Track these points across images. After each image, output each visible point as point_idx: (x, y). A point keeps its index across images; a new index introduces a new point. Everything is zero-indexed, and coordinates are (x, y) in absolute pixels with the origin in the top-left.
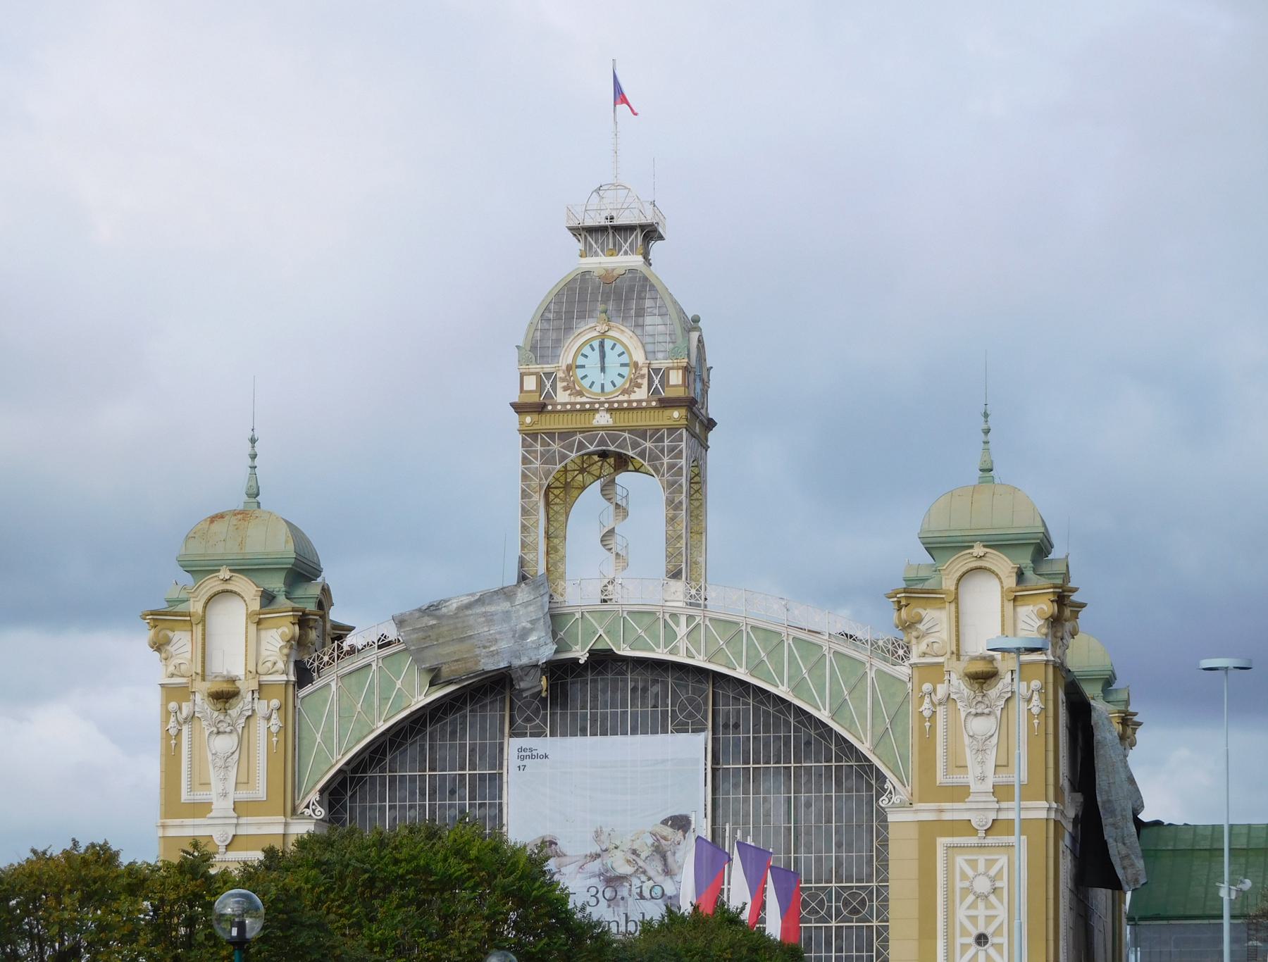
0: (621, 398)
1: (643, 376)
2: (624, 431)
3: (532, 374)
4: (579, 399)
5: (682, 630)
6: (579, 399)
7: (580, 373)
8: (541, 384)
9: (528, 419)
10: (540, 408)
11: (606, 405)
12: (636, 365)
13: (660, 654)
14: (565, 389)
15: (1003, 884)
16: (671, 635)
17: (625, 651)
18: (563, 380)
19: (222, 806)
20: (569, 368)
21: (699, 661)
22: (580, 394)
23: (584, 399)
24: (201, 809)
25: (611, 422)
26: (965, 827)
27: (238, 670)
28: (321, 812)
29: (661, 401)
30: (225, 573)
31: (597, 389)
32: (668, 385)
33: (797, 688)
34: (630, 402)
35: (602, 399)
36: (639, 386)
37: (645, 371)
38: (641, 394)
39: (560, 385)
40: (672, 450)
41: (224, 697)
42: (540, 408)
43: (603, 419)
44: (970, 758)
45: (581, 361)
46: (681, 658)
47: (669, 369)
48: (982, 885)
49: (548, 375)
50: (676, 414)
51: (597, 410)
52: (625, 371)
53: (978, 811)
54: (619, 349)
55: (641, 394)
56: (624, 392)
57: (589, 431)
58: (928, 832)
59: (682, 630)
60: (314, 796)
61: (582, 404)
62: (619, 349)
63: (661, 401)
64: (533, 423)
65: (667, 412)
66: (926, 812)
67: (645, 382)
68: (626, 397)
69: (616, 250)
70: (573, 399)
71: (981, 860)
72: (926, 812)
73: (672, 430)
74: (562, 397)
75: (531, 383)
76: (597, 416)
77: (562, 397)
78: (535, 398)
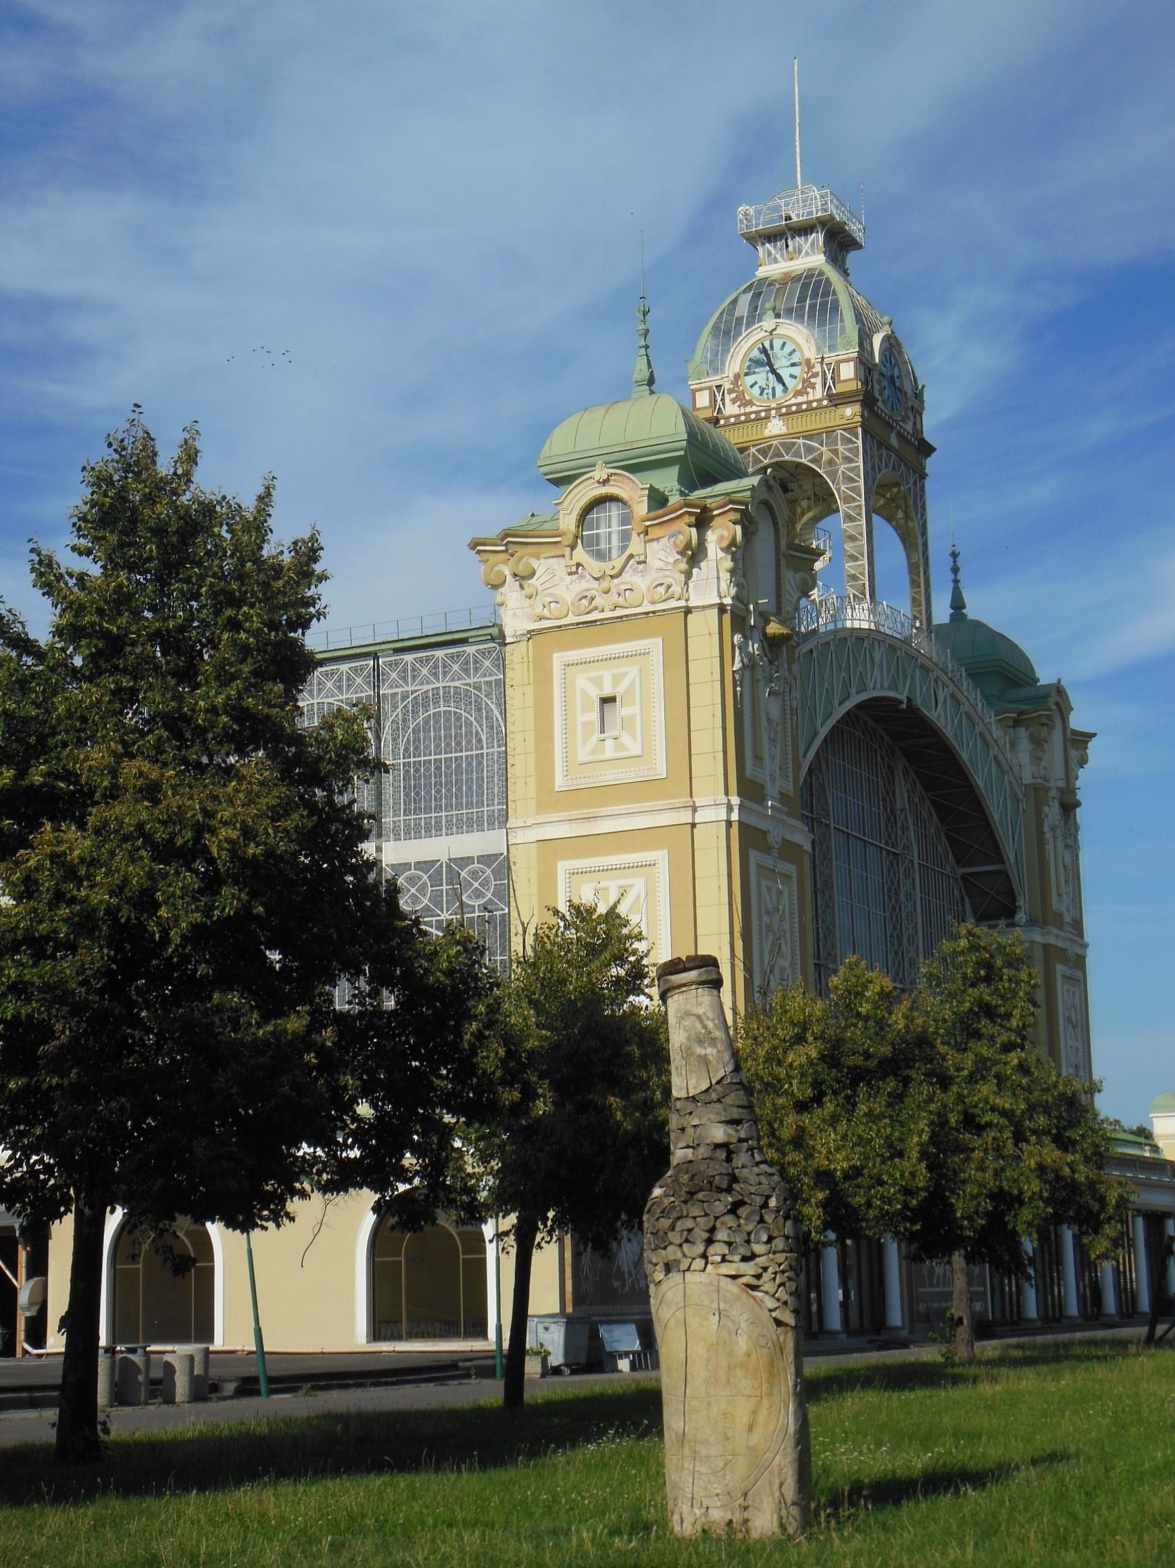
0: (793, 401)
1: (815, 375)
4: (748, 409)
6: (748, 409)
12: (808, 361)
14: (734, 401)
20: (737, 377)
22: (750, 403)
23: (755, 408)
25: (784, 430)
29: (830, 397)
32: (840, 381)
34: (809, 403)
39: (727, 398)
43: (776, 427)
47: (839, 363)
51: (767, 418)
52: (796, 371)
54: (788, 349)
56: (798, 393)
62: (788, 349)
65: (840, 410)
67: (818, 381)
68: (800, 399)
74: (731, 409)
77: (731, 409)
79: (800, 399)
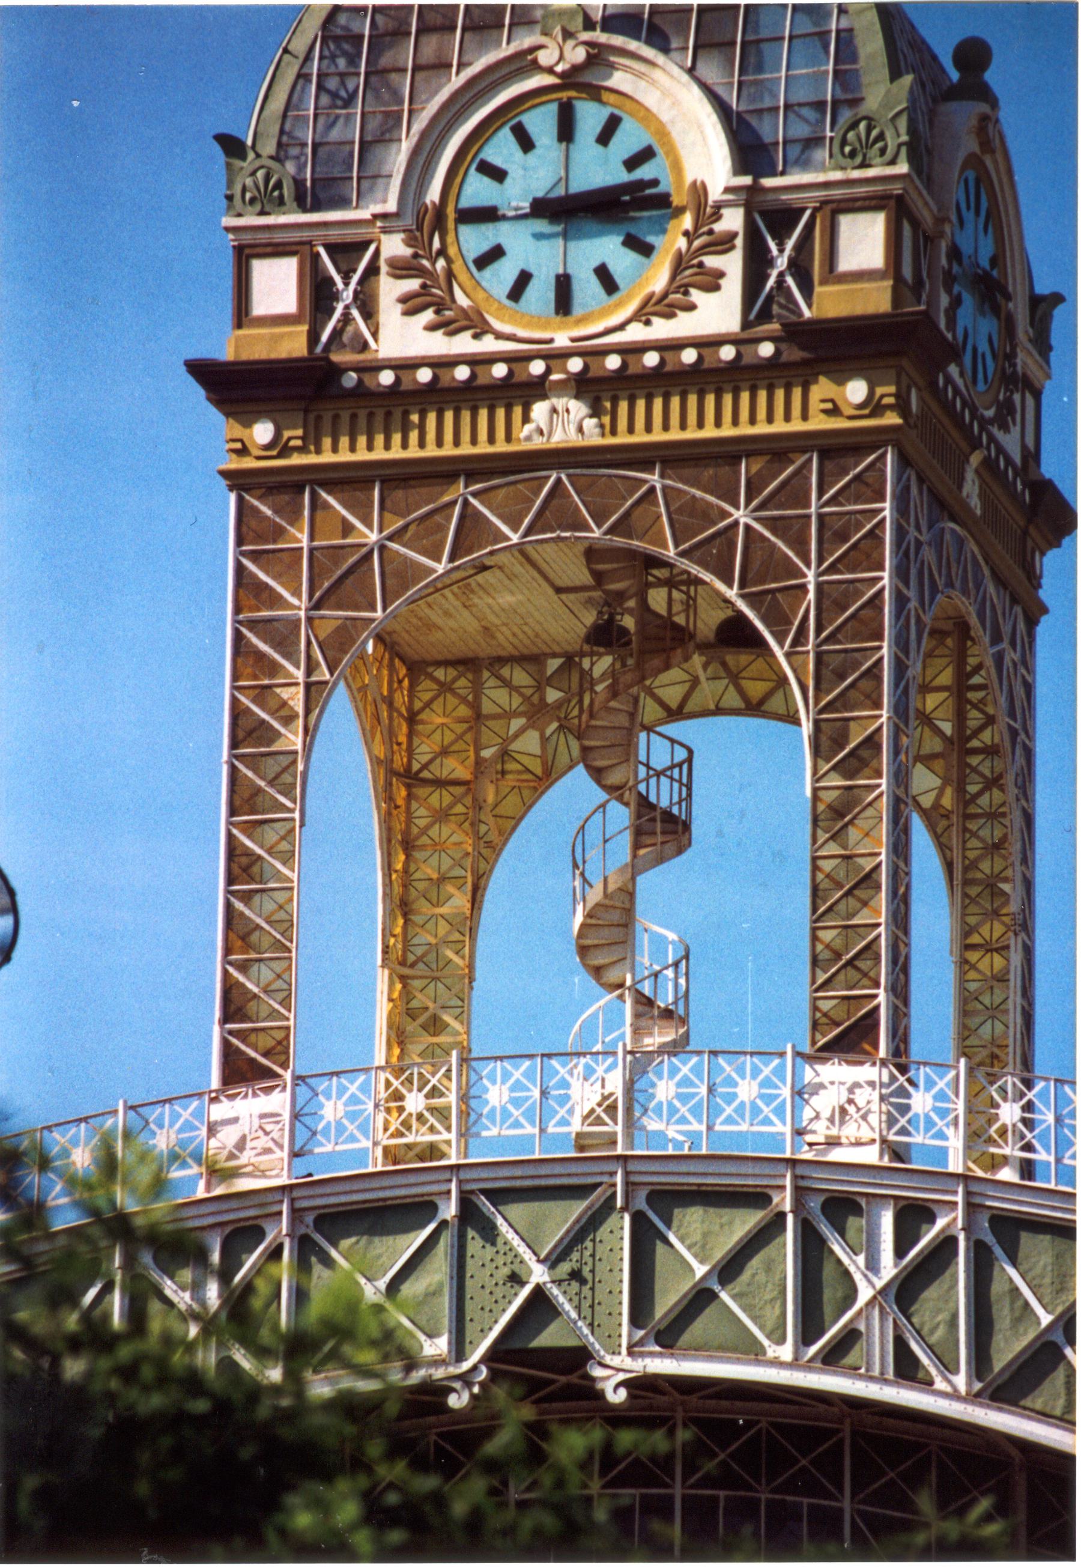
0: (636, 333)
1: (724, 244)
2: (646, 465)
3: (278, 251)
4: (464, 344)
6: (464, 344)
7: (473, 240)
8: (318, 295)
9: (263, 432)
11: (575, 365)
14: (411, 305)
18: (401, 269)
23: (489, 345)
25: (592, 435)
31: (540, 293)
32: (831, 273)
35: (562, 340)
36: (712, 282)
37: (733, 220)
38: (718, 312)
39: (390, 290)
40: (833, 531)
43: (561, 422)
45: (477, 190)
49: (346, 251)
50: (856, 390)
51: (538, 388)
55: (718, 312)
61: (477, 361)
63: (797, 332)
64: (279, 447)
65: (822, 389)
67: (732, 265)
68: (662, 329)
70: (439, 345)
73: (835, 449)
74: (402, 336)
75: (276, 286)
76: (540, 410)
78: (293, 344)
79: (662, 329)
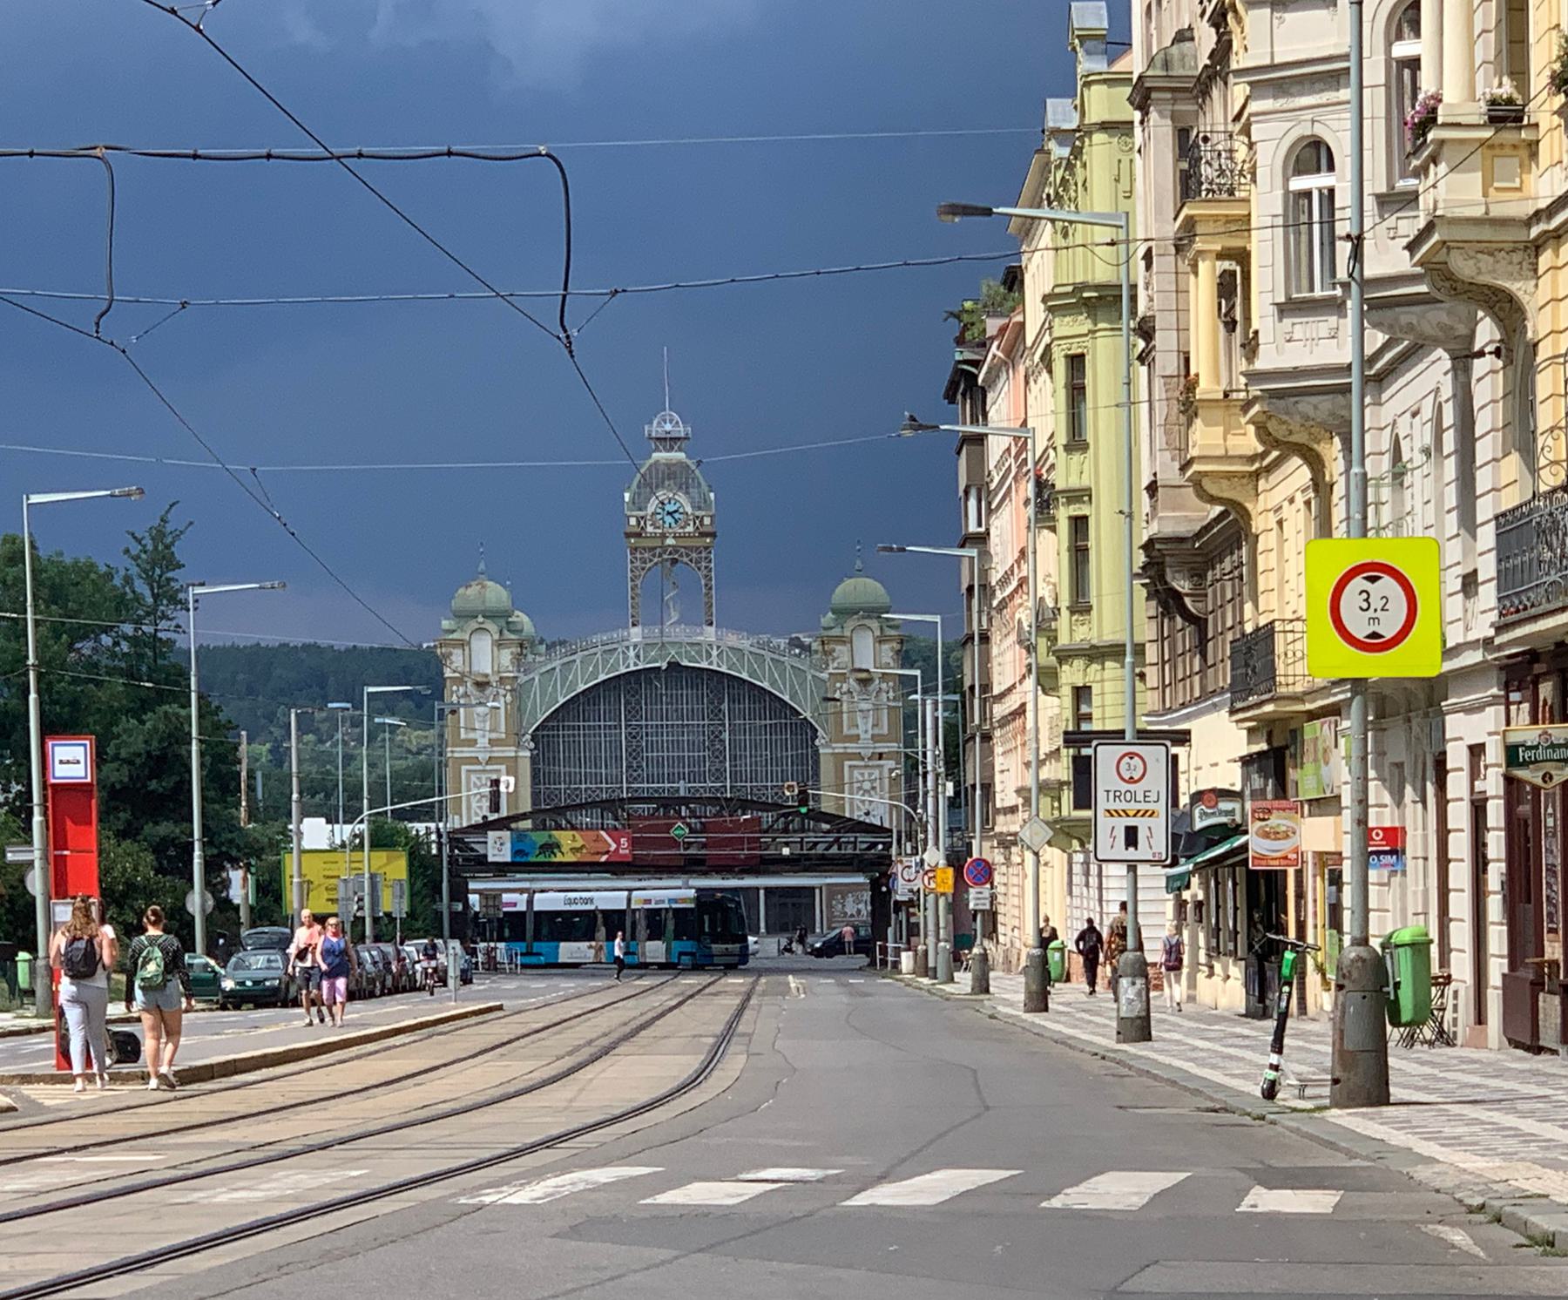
5: (715, 653)
10: (638, 535)
13: (704, 665)
15: (877, 784)
16: (709, 655)
17: (685, 663)
19: (483, 742)
21: (724, 669)
24: (473, 743)
26: (860, 757)
27: (489, 671)
28: (532, 745)
30: (480, 619)
33: (773, 683)
38: (690, 529)
41: (482, 685)
42: (638, 535)
44: (859, 721)
46: (714, 667)
48: (867, 786)
53: (865, 747)
57: (664, 548)
58: (840, 758)
59: (715, 653)
60: (528, 737)
66: (839, 748)
69: (671, 449)
71: (866, 772)
72: (839, 748)
77: (650, 529)
